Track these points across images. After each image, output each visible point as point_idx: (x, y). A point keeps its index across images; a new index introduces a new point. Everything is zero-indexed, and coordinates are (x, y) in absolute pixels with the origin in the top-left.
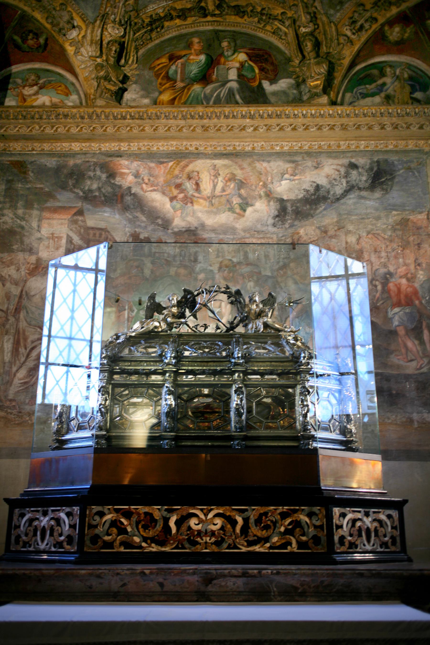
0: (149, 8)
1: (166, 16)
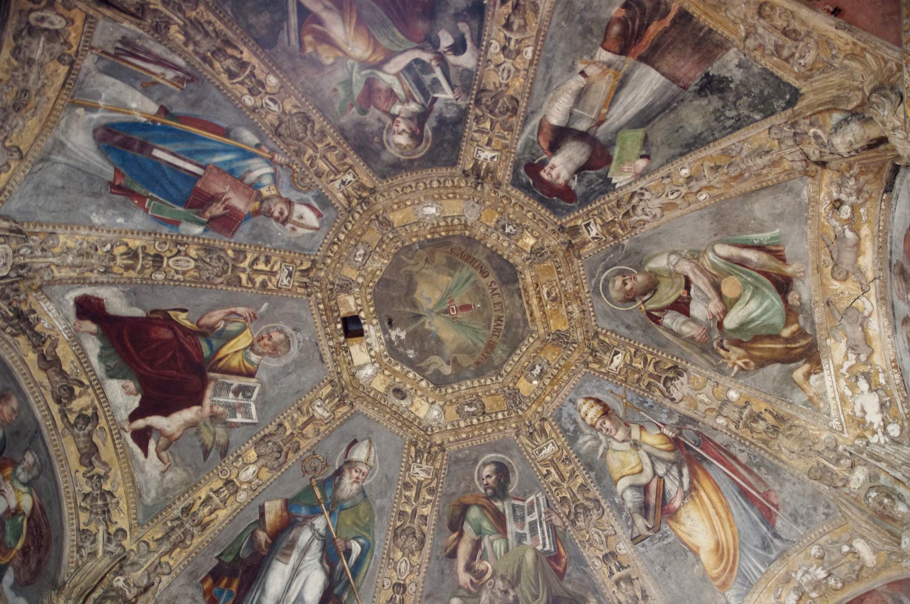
0: (48, 303)
1: (38, 335)
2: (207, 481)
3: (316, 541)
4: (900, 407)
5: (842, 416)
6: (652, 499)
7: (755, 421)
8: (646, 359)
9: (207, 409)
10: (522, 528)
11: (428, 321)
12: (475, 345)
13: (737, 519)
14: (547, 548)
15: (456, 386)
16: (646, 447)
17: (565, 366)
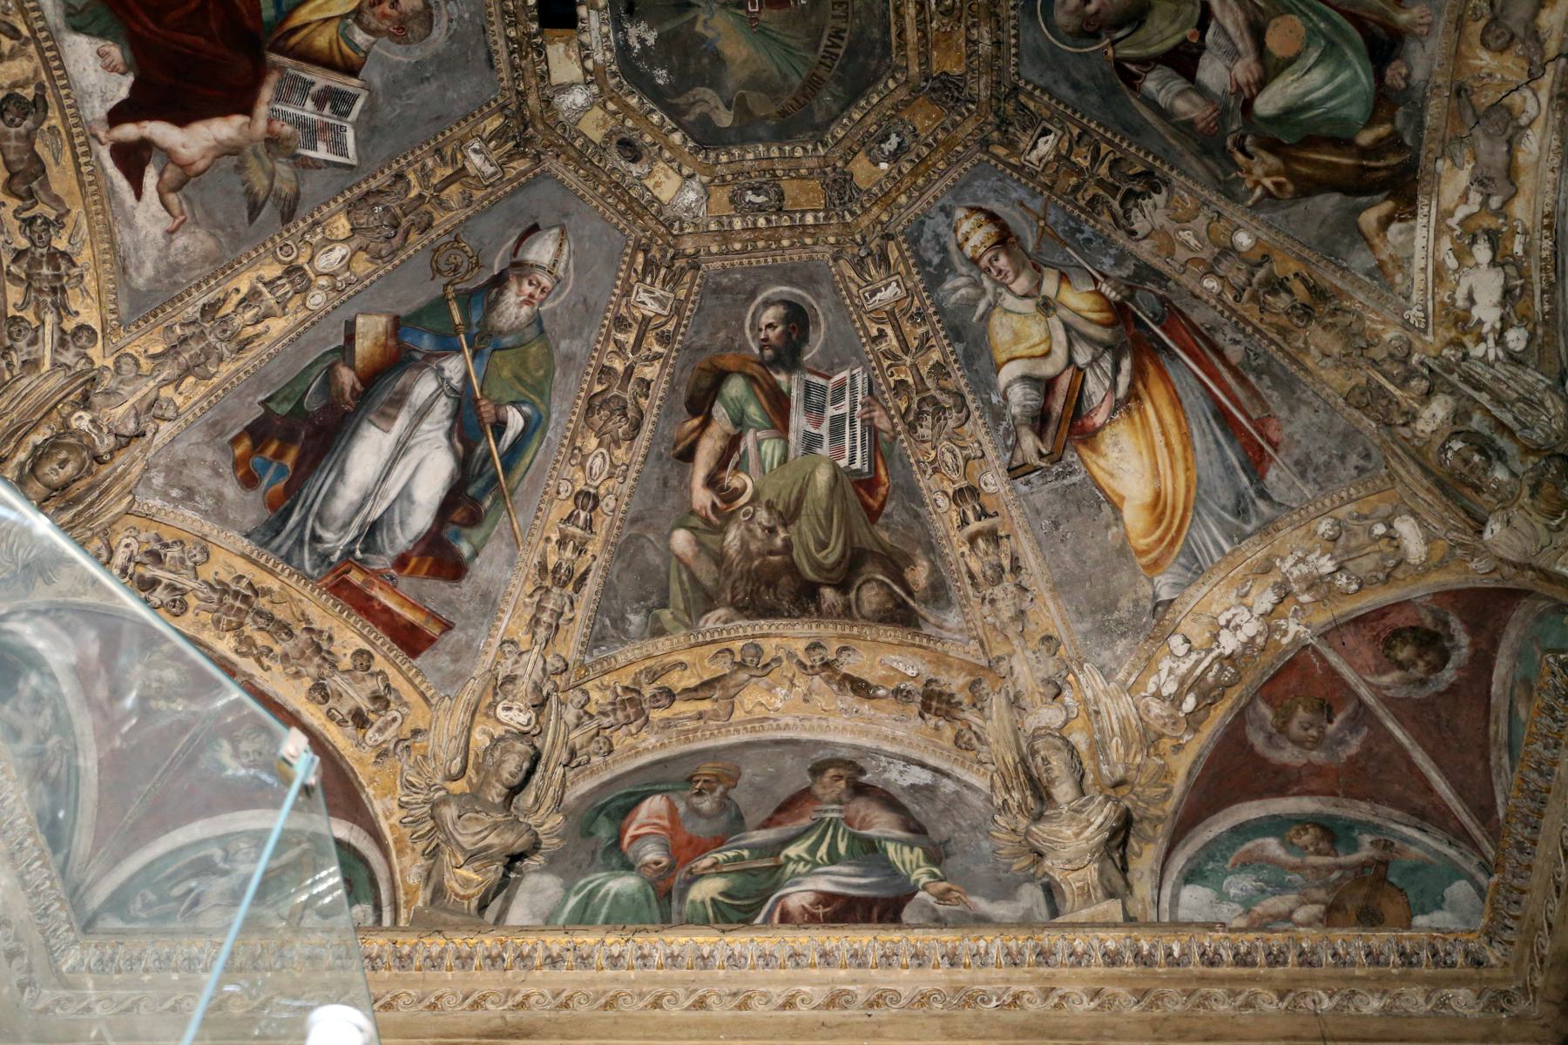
2: (253, 263)
3: (444, 399)
4: (1537, 299)
5: (1430, 304)
6: (1058, 406)
7: (1274, 293)
8: (1098, 150)
9: (261, 125)
10: (818, 425)
11: (702, 17)
12: (785, 77)
13: (1201, 457)
14: (857, 465)
15: (736, 152)
16: (1063, 312)
17: (944, 143)
